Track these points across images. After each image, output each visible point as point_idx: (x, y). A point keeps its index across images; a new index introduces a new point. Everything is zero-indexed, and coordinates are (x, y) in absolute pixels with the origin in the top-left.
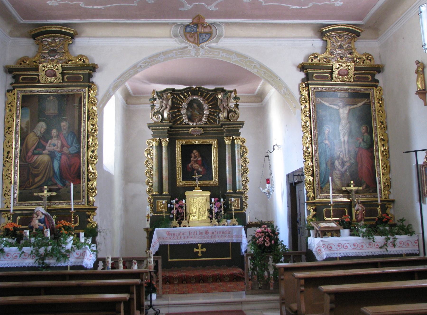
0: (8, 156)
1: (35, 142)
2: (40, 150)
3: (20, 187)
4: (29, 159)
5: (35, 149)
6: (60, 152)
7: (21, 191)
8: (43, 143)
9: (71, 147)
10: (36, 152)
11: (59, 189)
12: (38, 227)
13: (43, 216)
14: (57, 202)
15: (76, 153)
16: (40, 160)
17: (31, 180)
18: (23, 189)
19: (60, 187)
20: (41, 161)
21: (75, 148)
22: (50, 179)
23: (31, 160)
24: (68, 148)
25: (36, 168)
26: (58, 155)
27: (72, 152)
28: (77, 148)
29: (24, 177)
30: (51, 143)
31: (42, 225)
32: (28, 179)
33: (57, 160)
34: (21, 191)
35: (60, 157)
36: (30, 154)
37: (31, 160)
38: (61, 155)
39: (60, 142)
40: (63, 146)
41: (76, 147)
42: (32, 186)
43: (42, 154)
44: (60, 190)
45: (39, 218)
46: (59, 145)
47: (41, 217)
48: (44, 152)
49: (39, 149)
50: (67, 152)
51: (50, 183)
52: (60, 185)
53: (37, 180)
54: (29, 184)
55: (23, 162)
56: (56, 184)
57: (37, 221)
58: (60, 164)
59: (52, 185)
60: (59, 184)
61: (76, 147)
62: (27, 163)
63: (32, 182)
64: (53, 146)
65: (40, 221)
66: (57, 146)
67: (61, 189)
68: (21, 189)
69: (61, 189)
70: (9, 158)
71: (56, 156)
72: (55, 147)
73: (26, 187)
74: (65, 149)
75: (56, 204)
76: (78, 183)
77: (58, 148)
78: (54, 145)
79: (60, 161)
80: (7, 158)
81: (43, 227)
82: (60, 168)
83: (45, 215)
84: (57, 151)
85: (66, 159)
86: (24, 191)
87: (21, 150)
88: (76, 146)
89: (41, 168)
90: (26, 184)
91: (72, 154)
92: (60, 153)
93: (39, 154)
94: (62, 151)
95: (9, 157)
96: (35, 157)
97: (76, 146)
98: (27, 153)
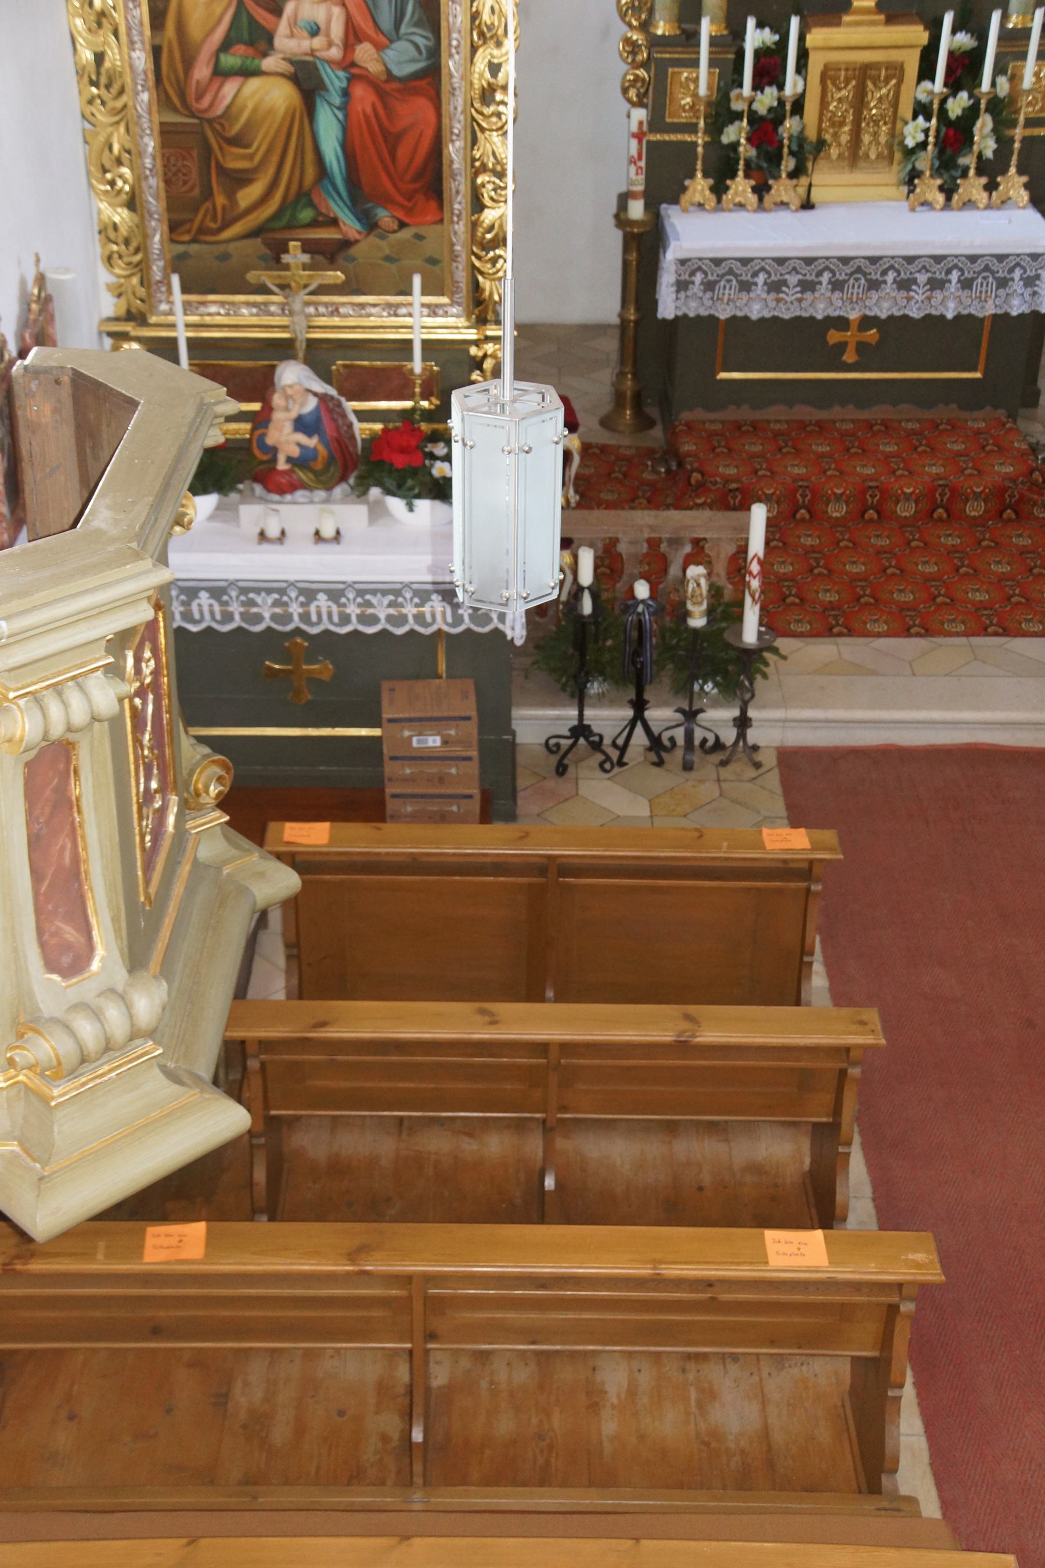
0: (98, 73)
1: (218, 9)
2: (250, 51)
3: (173, 227)
4: (199, 97)
5: (226, 46)
6: (345, 69)
7: (180, 248)
8: (262, 16)
9: (391, 41)
10: (229, 60)
11: (346, 244)
12: (296, 452)
13: (312, 403)
14: (343, 304)
15: (416, 76)
16: (250, 105)
17: (220, 200)
18: (186, 238)
19: (353, 235)
20: (255, 110)
21: (413, 52)
22: (303, 197)
23: (212, 105)
24: (379, 47)
25: (237, 141)
26: (335, 80)
27: (397, 71)
28: (420, 52)
29: (185, 183)
30: (294, 22)
31: (312, 442)
32: (208, 194)
33: (330, 104)
34: (180, 248)
35: (346, 93)
36: (202, 72)
37: (212, 105)
38: (349, 80)
39: (337, 11)
40: (353, 35)
41: (417, 47)
42: (225, 226)
43: (257, 73)
44: (354, 251)
45: (294, 414)
46: (337, 30)
47: (303, 405)
48: (269, 63)
49: (241, 48)
50: (374, 67)
51: (306, 215)
52: (350, 225)
53: (248, 196)
54: (214, 218)
55: (175, 110)
56: (334, 222)
57: (288, 427)
58: (346, 129)
59: (314, 224)
60: (348, 222)
61: (417, 47)
62: (192, 115)
63: (224, 208)
64: (305, 34)
65: (301, 424)
66: (328, 35)
67: (357, 241)
68: (174, 237)
69: (357, 241)
70: (108, 87)
71: (325, 89)
72: (318, 42)
73: (202, 231)
74: (365, 54)
75: (337, 310)
76: (429, 218)
77: (330, 44)
78: (314, 31)
79: (346, 116)
80: (95, 84)
81: (315, 449)
82: (347, 146)
83: (323, 398)
84: (330, 62)
85: (374, 109)
86: (194, 248)
87: (156, 52)
88: (421, 41)
89: (260, 142)
90: (200, 216)
91: (399, 79)
92: (341, 74)
93: (247, 73)
94: (353, 64)
95: (103, 80)
96: (230, 88)
97: (421, 41)
98: (189, 63)
